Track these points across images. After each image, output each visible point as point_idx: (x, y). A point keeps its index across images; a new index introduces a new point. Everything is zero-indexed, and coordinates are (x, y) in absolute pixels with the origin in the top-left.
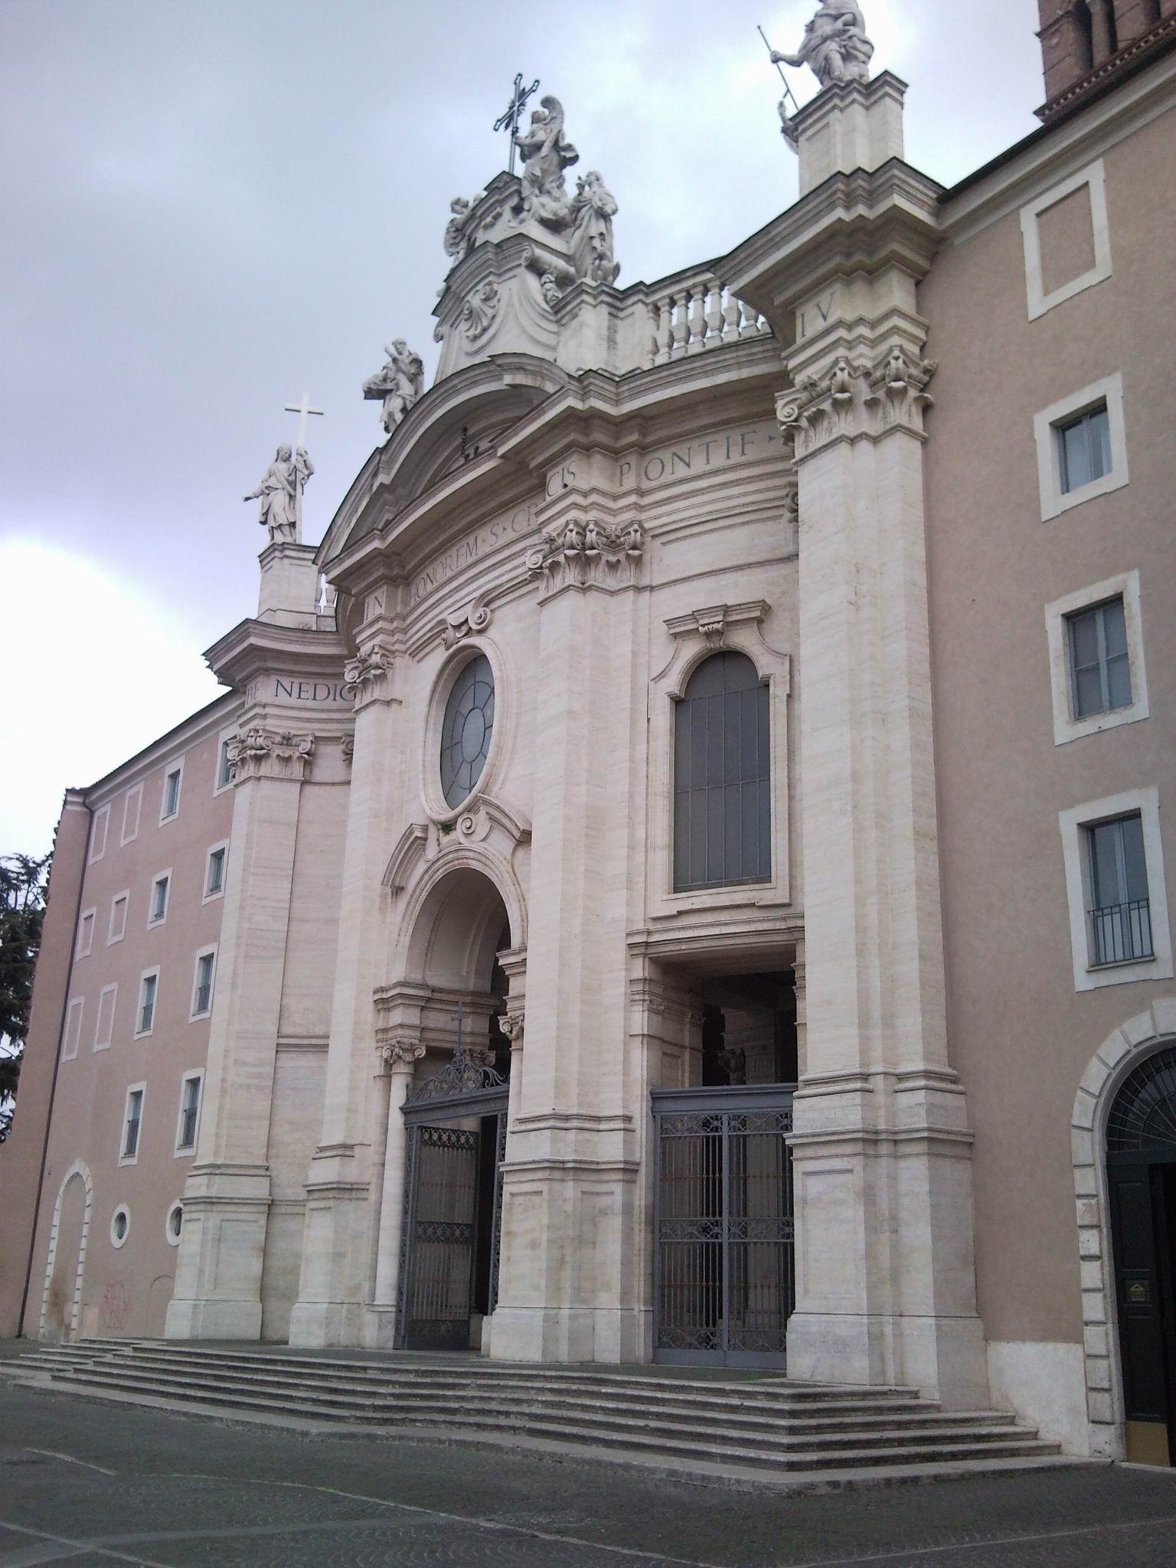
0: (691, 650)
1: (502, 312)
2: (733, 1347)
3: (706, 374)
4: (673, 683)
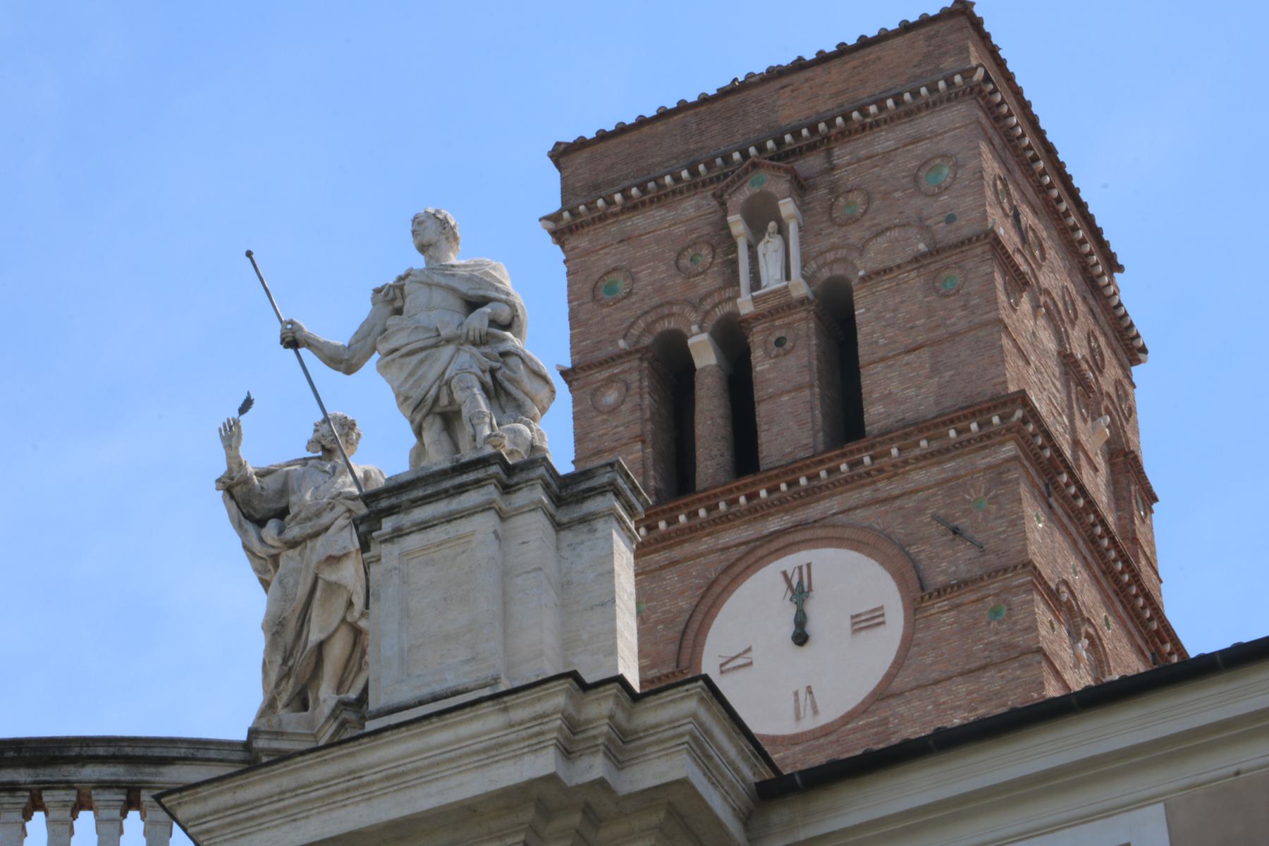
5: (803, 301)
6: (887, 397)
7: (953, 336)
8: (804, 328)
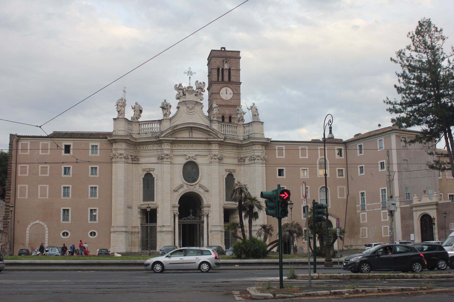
0: (228, 173)
1: (196, 111)
4: (226, 176)
8: (228, 71)
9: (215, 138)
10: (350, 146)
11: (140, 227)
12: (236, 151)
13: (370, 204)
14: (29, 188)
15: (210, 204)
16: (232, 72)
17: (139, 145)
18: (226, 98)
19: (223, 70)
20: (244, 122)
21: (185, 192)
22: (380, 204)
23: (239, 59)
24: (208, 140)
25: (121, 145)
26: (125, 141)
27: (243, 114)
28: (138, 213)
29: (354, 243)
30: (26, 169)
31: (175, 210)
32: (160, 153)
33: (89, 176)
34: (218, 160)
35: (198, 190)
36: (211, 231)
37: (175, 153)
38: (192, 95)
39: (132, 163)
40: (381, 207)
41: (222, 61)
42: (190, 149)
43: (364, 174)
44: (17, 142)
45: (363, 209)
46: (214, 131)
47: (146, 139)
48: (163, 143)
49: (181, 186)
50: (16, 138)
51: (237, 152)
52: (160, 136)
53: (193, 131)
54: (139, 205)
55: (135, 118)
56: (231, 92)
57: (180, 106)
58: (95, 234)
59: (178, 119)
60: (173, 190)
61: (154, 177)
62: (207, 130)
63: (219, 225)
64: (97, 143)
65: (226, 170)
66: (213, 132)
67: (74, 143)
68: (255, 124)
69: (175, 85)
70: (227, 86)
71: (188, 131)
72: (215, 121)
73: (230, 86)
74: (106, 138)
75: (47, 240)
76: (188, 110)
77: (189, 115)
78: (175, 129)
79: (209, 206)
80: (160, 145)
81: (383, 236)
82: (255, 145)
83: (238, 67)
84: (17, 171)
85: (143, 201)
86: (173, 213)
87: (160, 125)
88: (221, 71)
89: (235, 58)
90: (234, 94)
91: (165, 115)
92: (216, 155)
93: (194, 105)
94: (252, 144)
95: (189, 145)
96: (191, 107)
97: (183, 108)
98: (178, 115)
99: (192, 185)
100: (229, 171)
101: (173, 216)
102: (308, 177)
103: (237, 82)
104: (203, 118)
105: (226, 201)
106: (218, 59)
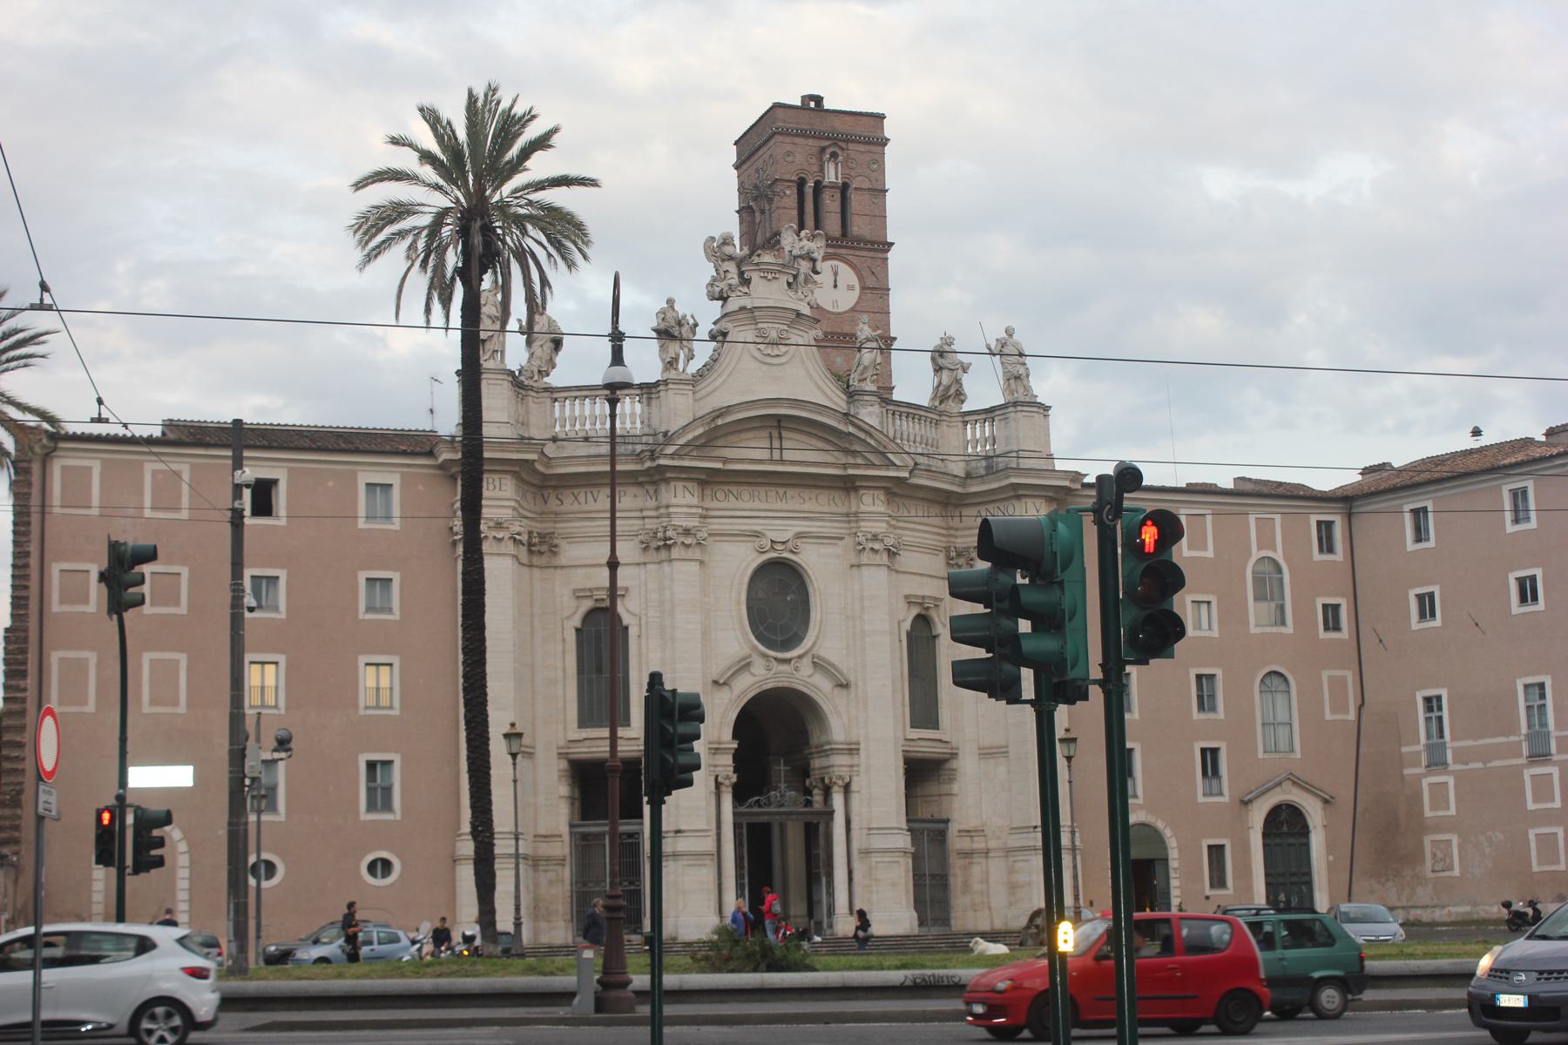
0: (915, 611)
2: (933, 926)
3: (941, 481)
4: (907, 625)
5: (837, 188)
6: (858, 226)
7: (875, 216)
8: (839, 195)
9: (879, 467)
10: (1360, 507)
11: (566, 838)
12: (937, 521)
13: (1470, 743)
14: (99, 664)
15: (854, 740)
16: (854, 198)
17: (555, 487)
18: (835, 303)
19: (818, 184)
20: (963, 402)
21: (758, 691)
22: (1521, 741)
23: (880, 148)
24: (851, 471)
25: (497, 483)
26: (517, 469)
27: (960, 372)
28: (559, 776)
29: (1399, 899)
30: (88, 578)
31: (718, 763)
32: (650, 524)
33: (361, 617)
34: (885, 558)
35: (809, 680)
36: (867, 852)
37: (716, 525)
38: (775, 283)
39: (531, 566)
40: (1525, 752)
41: (814, 150)
42: (774, 507)
43: (1438, 622)
44: (47, 457)
45: (1437, 762)
46: (871, 436)
47: (593, 464)
48: (667, 481)
49: (744, 666)
50: (45, 441)
51: (943, 524)
52: (662, 450)
53: (784, 434)
54: (562, 743)
55: (536, 370)
56: (855, 281)
57: (730, 326)
58: (387, 866)
59: (725, 381)
60: (710, 680)
61: (625, 622)
62: (844, 433)
63: (895, 825)
64: (389, 472)
65: (910, 601)
66: (869, 440)
67: (291, 472)
68: (1020, 414)
69: (707, 241)
70: (835, 254)
71: (765, 433)
72: (871, 393)
73: (850, 257)
74: (430, 454)
75: (183, 895)
76: (762, 349)
77: (765, 367)
78: (720, 422)
79: (852, 750)
80: (651, 489)
81: (1535, 868)
82: (1024, 500)
83: (877, 181)
84: (46, 590)
85: (579, 727)
86: (713, 778)
87: (649, 405)
88: (811, 191)
89: (868, 142)
90: (863, 288)
91: (671, 364)
92: (880, 537)
93: (785, 327)
94: (1012, 494)
95: (769, 493)
96: (774, 335)
97: (741, 333)
98: (725, 364)
99: (788, 661)
100: (921, 604)
101: (713, 788)
102: (1215, 633)
103: (874, 239)
104: (820, 383)
105: (912, 727)
106: (798, 140)
